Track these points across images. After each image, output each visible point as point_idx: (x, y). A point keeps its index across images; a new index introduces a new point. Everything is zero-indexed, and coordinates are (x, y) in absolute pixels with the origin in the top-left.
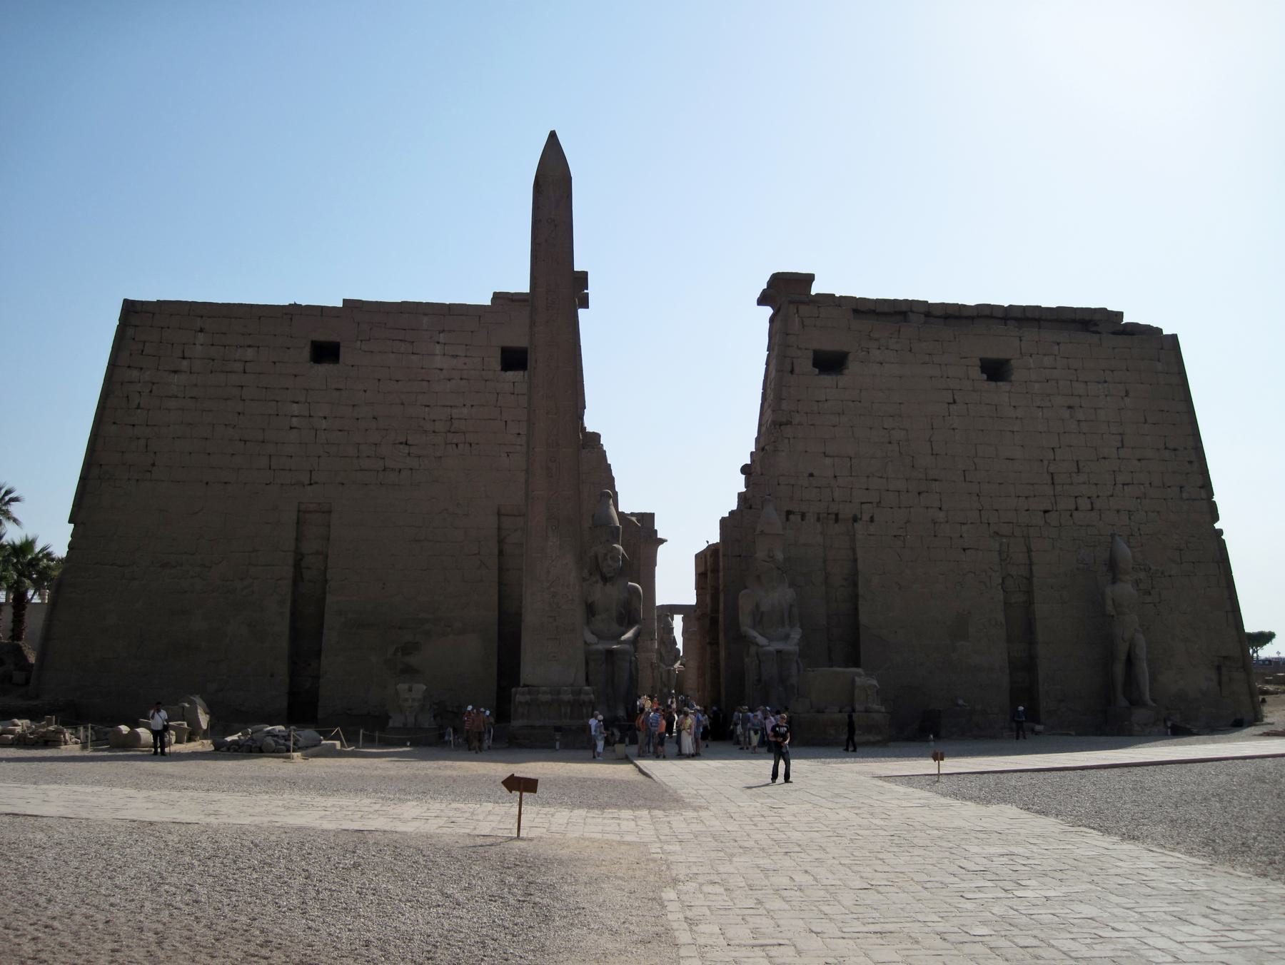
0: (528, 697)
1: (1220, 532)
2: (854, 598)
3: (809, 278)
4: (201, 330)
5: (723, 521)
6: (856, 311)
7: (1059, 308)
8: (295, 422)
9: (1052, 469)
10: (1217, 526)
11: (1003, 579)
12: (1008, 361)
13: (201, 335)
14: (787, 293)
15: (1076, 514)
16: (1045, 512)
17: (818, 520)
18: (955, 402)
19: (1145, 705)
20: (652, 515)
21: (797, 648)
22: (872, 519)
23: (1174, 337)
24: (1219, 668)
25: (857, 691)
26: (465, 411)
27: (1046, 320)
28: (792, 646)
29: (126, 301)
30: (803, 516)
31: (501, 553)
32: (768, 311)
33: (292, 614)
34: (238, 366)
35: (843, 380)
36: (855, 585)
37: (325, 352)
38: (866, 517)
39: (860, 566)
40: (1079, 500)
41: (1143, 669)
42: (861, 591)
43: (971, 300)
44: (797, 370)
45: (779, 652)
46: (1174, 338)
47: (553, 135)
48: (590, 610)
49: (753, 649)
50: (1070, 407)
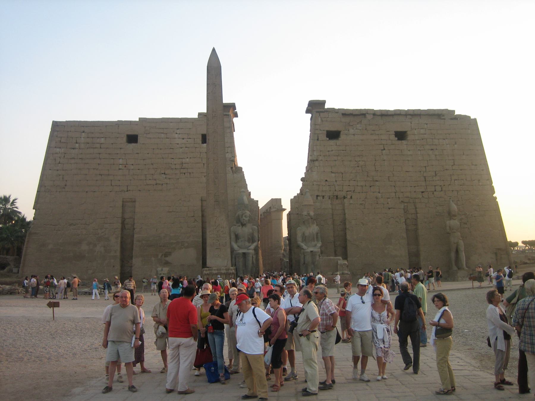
0: (208, 272)
1: (496, 198)
2: (345, 229)
4: (83, 132)
5: (291, 200)
6: (343, 114)
7: (428, 110)
9: (425, 175)
11: (405, 220)
13: (83, 134)
14: (315, 108)
15: (435, 192)
16: (422, 192)
17: (329, 198)
19: (464, 269)
20: (280, 199)
21: (319, 250)
22: (351, 197)
24: (496, 254)
25: (339, 266)
26: (187, 160)
27: (423, 115)
28: (317, 250)
30: (323, 197)
31: (203, 216)
32: (310, 115)
33: (121, 242)
35: (338, 142)
36: (345, 224)
37: (132, 139)
38: (349, 197)
40: (437, 187)
41: (463, 255)
43: (392, 109)
45: (312, 252)
47: (214, 50)
48: (237, 237)
49: (302, 251)
50: (432, 150)
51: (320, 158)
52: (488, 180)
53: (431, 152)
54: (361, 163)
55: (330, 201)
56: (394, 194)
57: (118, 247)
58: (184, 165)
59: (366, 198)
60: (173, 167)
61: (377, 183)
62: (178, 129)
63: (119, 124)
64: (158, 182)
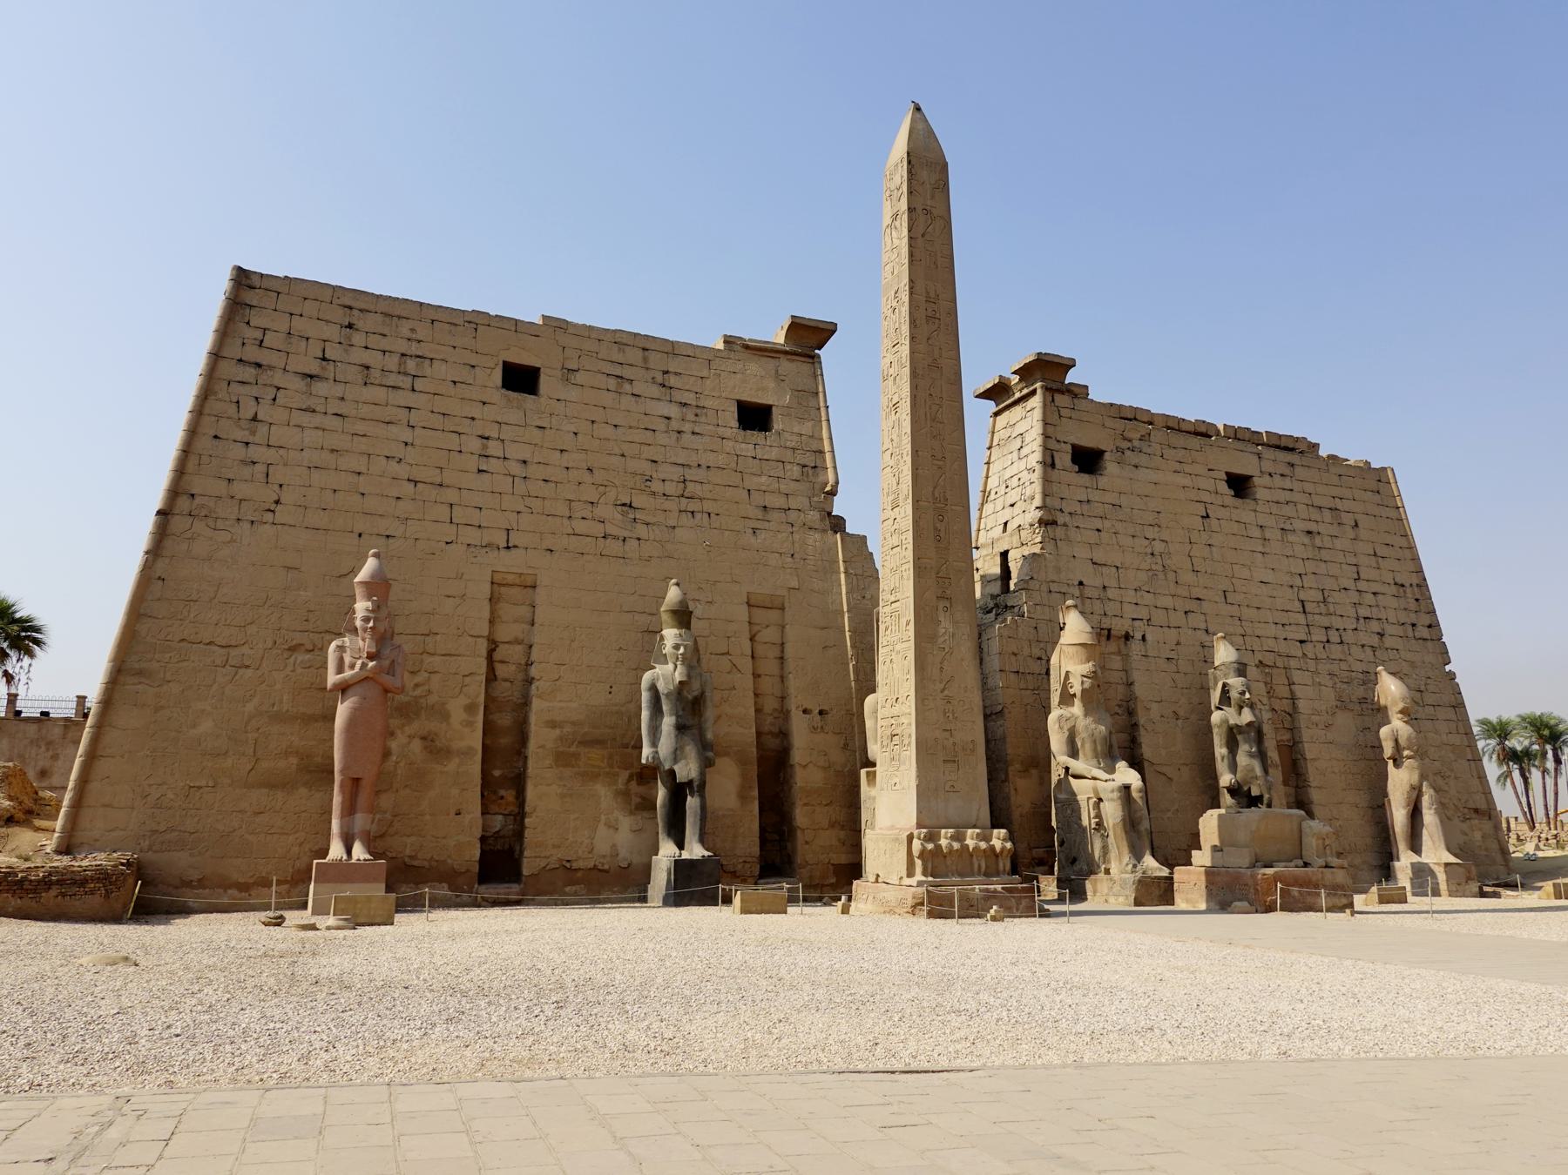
1: (1452, 676)
3: (1066, 365)
4: (350, 326)
12: (1248, 478)
16: (1302, 642)
26: (701, 474)
35: (1103, 481)
36: (1131, 713)
37: (521, 379)
38: (1138, 636)
39: (1139, 690)
40: (1331, 633)
42: (1142, 719)
44: (1057, 461)
52: (1430, 626)
53: (1306, 540)
54: (1158, 547)
57: (475, 740)
58: (690, 486)
59: (1178, 644)
60: (656, 486)
62: (667, 372)
63: (476, 322)
64: (612, 530)
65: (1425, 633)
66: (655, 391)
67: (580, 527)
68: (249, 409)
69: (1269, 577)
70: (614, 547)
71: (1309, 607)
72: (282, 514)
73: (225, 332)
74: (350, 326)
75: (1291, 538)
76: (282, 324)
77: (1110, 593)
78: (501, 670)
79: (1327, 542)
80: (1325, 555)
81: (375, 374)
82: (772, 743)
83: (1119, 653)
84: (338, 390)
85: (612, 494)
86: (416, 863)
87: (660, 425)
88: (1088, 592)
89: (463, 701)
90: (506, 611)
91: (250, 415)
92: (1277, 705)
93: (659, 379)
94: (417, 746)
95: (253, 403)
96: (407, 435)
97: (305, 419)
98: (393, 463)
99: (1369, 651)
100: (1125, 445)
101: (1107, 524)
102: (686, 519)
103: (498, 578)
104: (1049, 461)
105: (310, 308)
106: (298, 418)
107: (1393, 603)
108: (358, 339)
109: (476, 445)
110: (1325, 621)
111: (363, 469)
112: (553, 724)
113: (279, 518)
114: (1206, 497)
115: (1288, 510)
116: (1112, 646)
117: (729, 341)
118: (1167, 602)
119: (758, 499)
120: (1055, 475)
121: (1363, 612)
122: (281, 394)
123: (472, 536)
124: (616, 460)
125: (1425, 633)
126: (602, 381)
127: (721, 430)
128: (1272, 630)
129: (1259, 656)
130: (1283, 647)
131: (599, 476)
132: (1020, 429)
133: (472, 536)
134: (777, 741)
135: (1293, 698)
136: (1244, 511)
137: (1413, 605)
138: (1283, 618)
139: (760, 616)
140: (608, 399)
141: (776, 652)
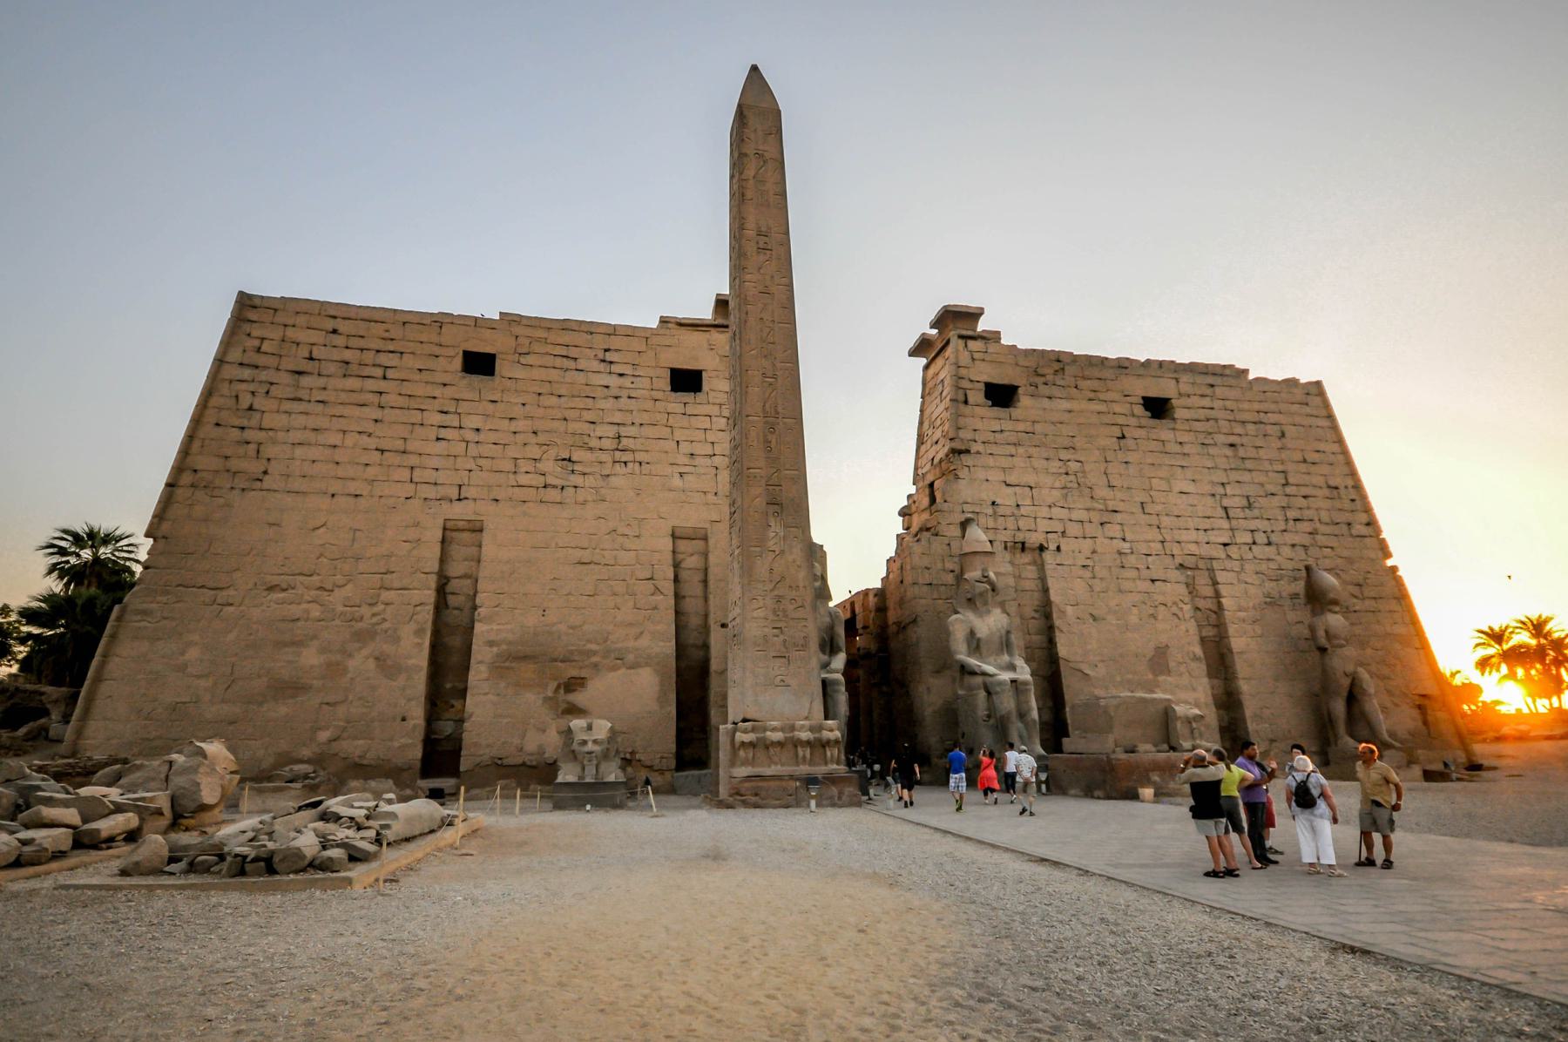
1: (1394, 569)
4: (335, 331)
8: (443, 433)
9: (1226, 502)
10: (1389, 563)
12: (1167, 401)
16: (1225, 545)
18: (1124, 437)
22: (1058, 548)
23: (1318, 384)
26: (632, 431)
29: (241, 294)
31: (676, 580)
34: (379, 372)
35: (1015, 412)
36: (1048, 616)
37: (479, 364)
38: (1053, 547)
39: (1054, 597)
42: (1057, 622)
46: (1318, 384)
51: (974, 448)
52: (1368, 524)
53: (1229, 452)
54: (1073, 466)
55: (1008, 556)
56: (1159, 546)
57: (421, 660)
58: (624, 442)
59: (1094, 552)
60: (594, 443)
61: (1118, 517)
63: (440, 321)
64: (551, 480)
65: (1364, 530)
66: (596, 365)
67: (523, 479)
68: (246, 401)
69: (1190, 488)
70: (553, 494)
71: (1231, 514)
72: (268, 482)
73: (227, 342)
74: (335, 331)
75: (1212, 450)
76: (276, 334)
77: (1023, 511)
78: (452, 600)
79: (1252, 453)
80: (1249, 464)
81: (354, 369)
82: (697, 654)
83: (1034, 563)
84: (321, 382)
85: (553, 452)
86: (365, 762)
87: (599, 392)
88: (1001, 511)
89: (413, 626)
90: (457, 552)
91: (246, 405)
92: (1201, 604)
93: (601, 356)
94: (371, 664)
95: (249, 396)
96: (378, 414)
97: (296, 406)
98: (365, 437)
99: (1300, 550)
100: (1040, 380)
101: (1021, 450)
102: (619, 468)
103: (449, 525)
104: (961, 398)
105: (301, 320)
106: (287, 406)
107: (1327, 504)
108: (339, 340)
109: (438, 419)
110: (1253, 524)
111: (338, 443)
112: (491, 644)
113: (265, 485)
114: (1121, 420)
115: (1208, 426)
116: (1027, 558)
117: (664, 321)
118: (1083, 515)
119: (685, 448)
120: (967, 410)
121: (1291, 514)
122: (273, 388)
123: (430, 492)
124: (560, 426)
125: (1364, 530)
126: (549, 361)
127: (656, 394)
128: (1193, 535)
129: (1178, 560)
130: (1205, 551)
131: (542, 438)
132: (941, 376)
133: (430, 492)
134: (702, 653)
135: (1218, 595)
136: (1163, 430)
137: (1347, 505)
138: (1207, 524)
139: (683, 546)
140: (554, 375)
141: (700, 576)
